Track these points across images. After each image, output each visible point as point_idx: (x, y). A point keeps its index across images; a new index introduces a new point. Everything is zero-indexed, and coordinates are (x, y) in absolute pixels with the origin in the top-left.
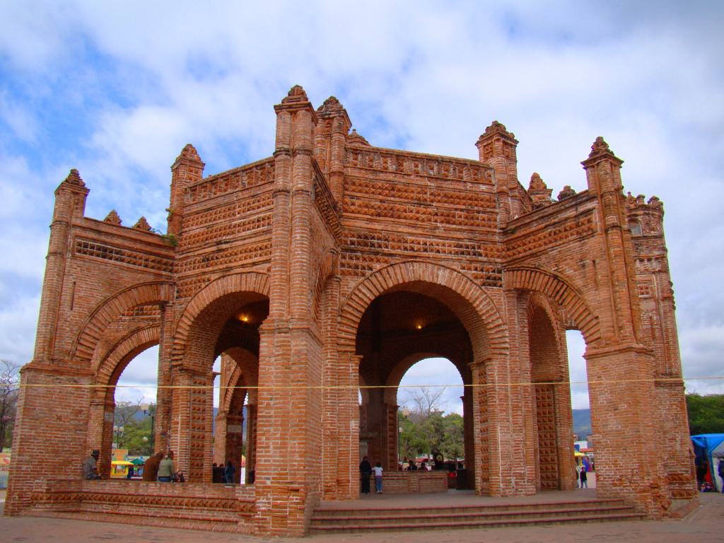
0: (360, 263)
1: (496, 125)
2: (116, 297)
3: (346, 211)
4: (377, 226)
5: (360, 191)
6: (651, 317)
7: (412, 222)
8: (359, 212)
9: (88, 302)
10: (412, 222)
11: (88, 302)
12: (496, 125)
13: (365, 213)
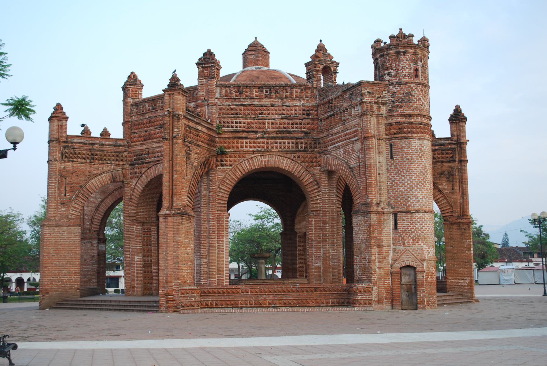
0: (138, 171)
1: (209, 51)
2: (106, 198)
3: (132, 142)
4: (144, 147)
5: (137, 129)
6: (359, 157)
7: (158, 140)
8: (137, 141)
9: (94, 203)
10: (158, 140)
11: (94, 203)
12: (209, 51)
13: (139, 141)
